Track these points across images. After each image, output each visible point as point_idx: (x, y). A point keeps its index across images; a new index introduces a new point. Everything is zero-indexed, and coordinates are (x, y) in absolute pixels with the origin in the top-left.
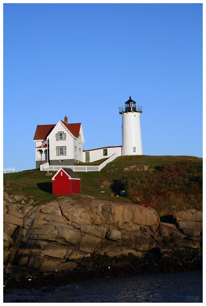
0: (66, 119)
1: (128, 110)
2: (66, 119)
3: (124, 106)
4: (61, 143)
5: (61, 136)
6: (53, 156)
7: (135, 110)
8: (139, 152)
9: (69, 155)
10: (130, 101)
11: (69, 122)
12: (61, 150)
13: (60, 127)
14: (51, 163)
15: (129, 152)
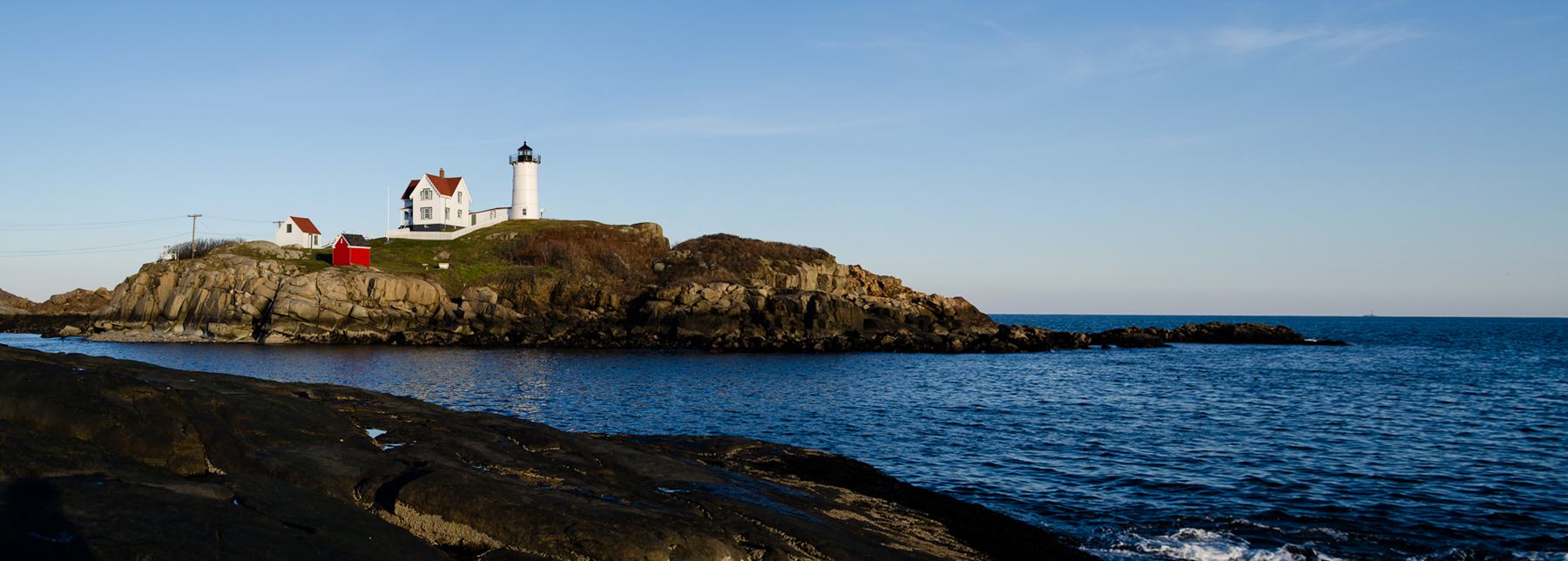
0: (442, 172)
1: (521, 159)
2: (442, 172)
3: (515, 154)
4: (426, 204)
5: (426, 192)
6: (417, 221)
7: (530, 159)
8: (532, 215)
9: (438, 218)
10: (525, 148)
11: (447, 176)
12: (427, 212)
13: (424, 184)
14: (412, 228)
15: (519, 216)
